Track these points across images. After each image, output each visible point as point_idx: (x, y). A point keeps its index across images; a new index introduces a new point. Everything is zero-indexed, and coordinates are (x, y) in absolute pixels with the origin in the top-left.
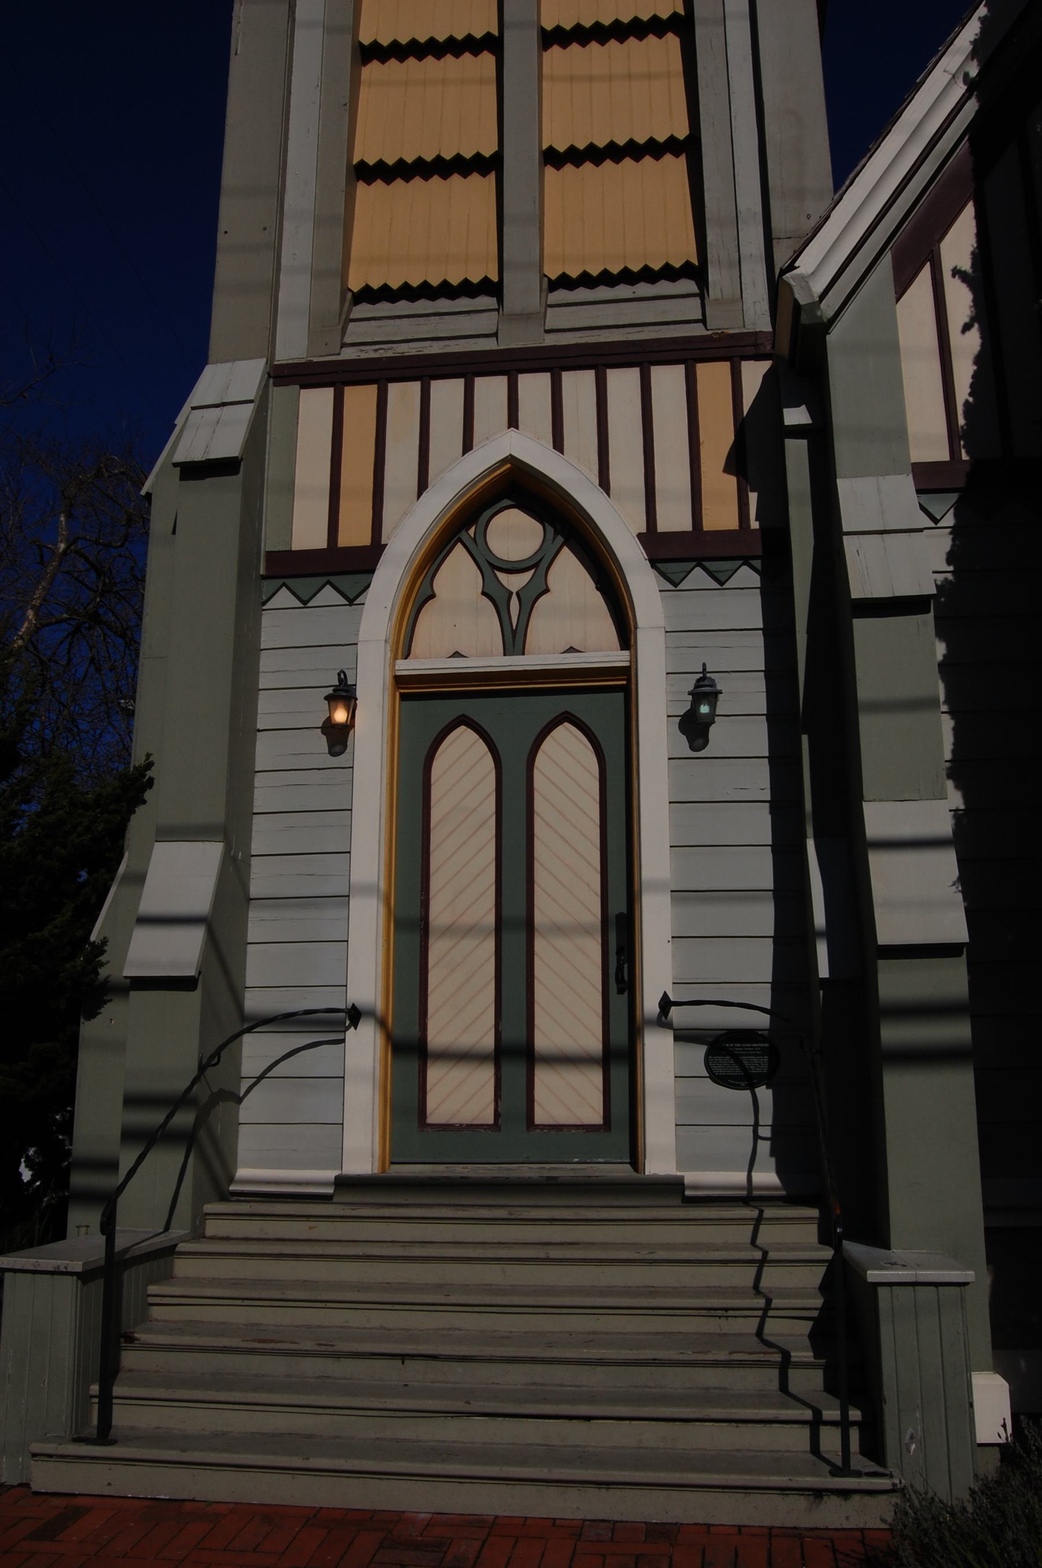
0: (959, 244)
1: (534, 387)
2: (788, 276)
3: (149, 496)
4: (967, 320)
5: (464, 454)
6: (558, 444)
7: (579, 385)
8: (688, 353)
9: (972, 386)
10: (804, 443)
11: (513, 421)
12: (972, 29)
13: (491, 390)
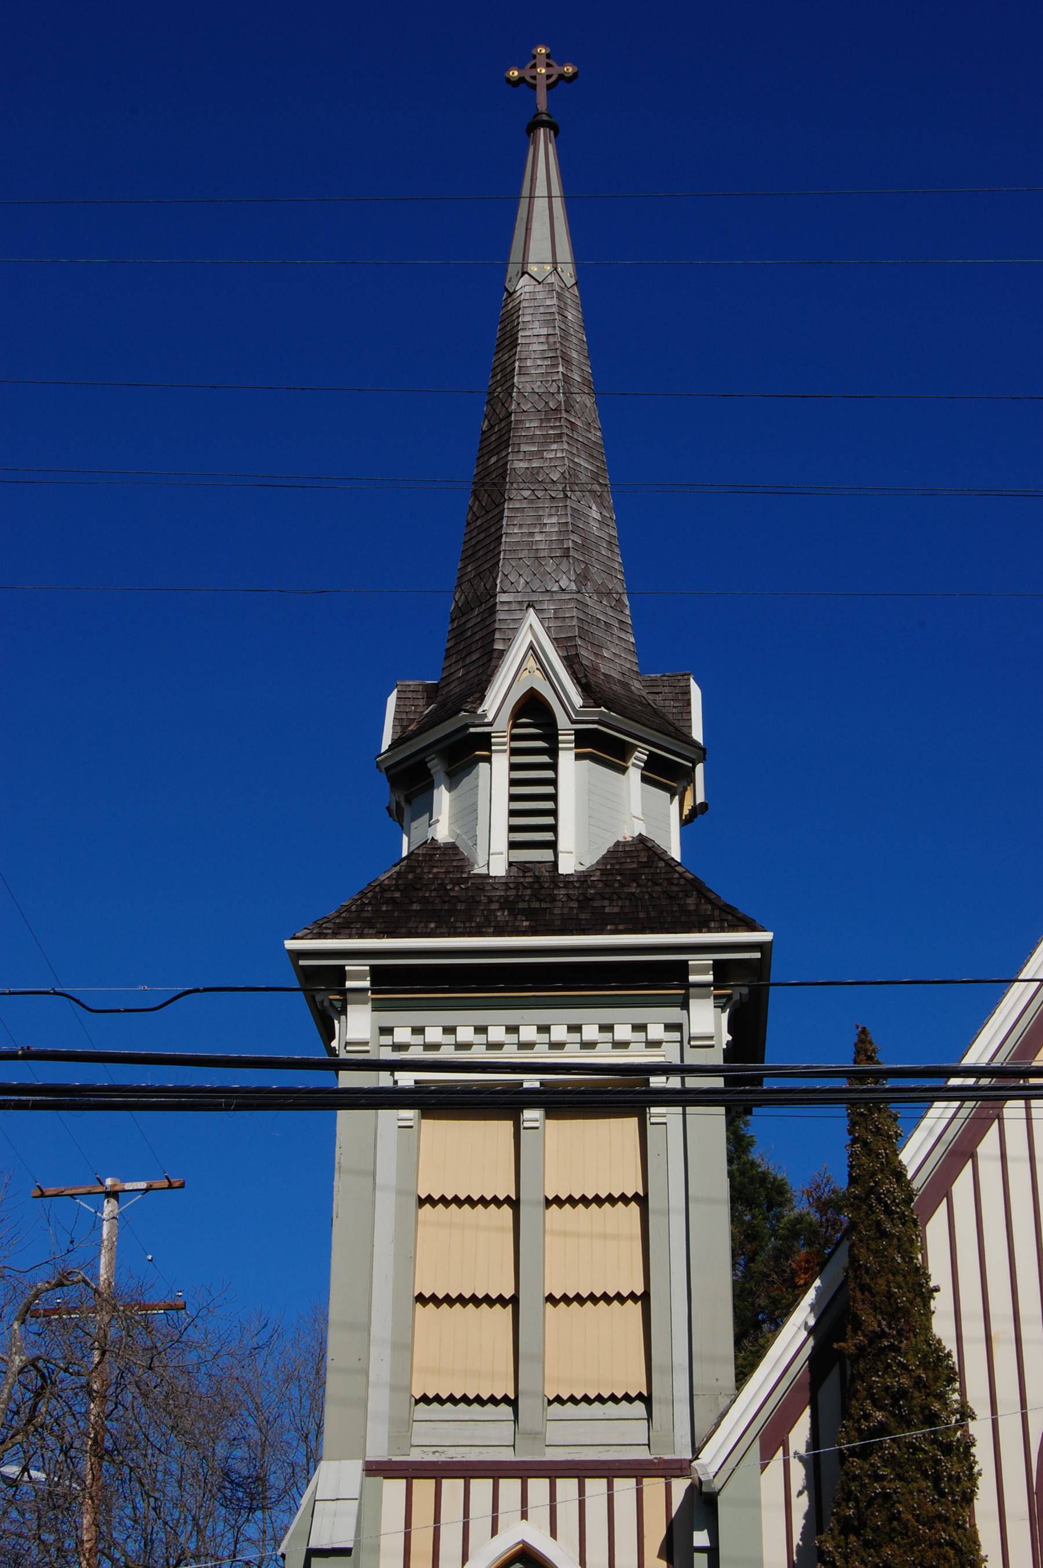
0: (800, 1435)
1: (539, 1487)
2: (694, 1464)
3: (283, 1556)
4: (801, 1488)
5: (492, 1536)
6: (553, 1534)
7: (567, 1487)
8: (638, 1470)
9: (802, 1534)
10: (705, 1556)
11: (524, 1516)
12: (810, 1296)
13: (510, 1488)
